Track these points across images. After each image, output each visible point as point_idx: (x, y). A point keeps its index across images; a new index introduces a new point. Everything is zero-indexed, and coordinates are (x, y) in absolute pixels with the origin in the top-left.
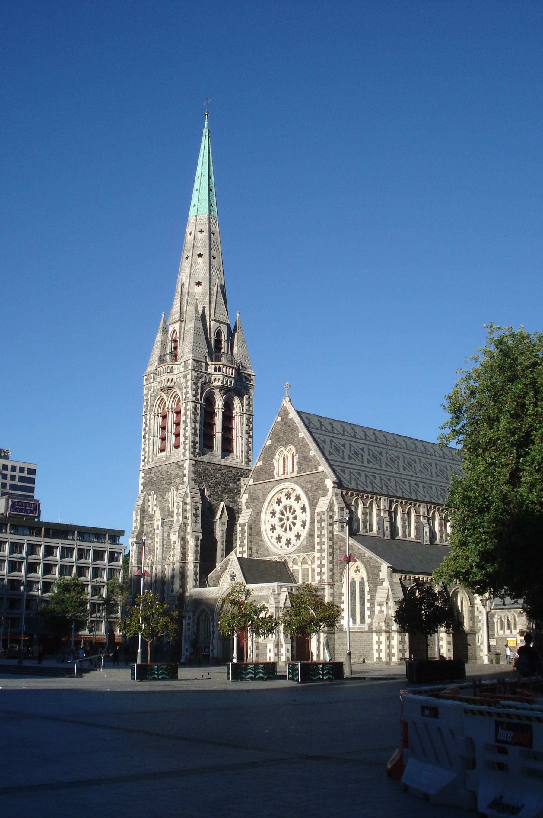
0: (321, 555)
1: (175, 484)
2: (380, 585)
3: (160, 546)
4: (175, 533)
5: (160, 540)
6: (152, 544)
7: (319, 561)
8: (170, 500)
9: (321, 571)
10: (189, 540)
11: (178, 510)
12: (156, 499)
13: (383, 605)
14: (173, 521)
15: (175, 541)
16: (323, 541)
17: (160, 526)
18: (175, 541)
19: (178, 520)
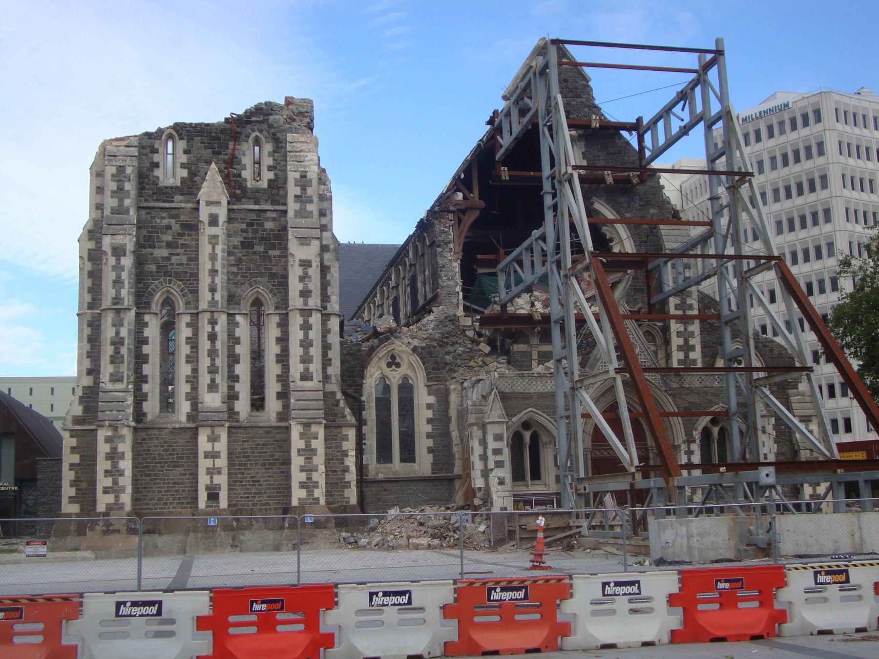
0: (686, 329)
1: (265, 126)
2: (792, 388)
3: (223, 267)
4: (307, 242)
5: (223, 251)
6: (174, 259)
7: (682, 339)
8: (247, 160)
9: (686, 356)
10: (326, 263)
11: (304, 189)
12: (186, 152)
13: (811, 421)
14: (286, 212)
15: (310, 261)
16: (689, 301)
17: (223, 217)
18: (310, 261)
19: (300, 214)
